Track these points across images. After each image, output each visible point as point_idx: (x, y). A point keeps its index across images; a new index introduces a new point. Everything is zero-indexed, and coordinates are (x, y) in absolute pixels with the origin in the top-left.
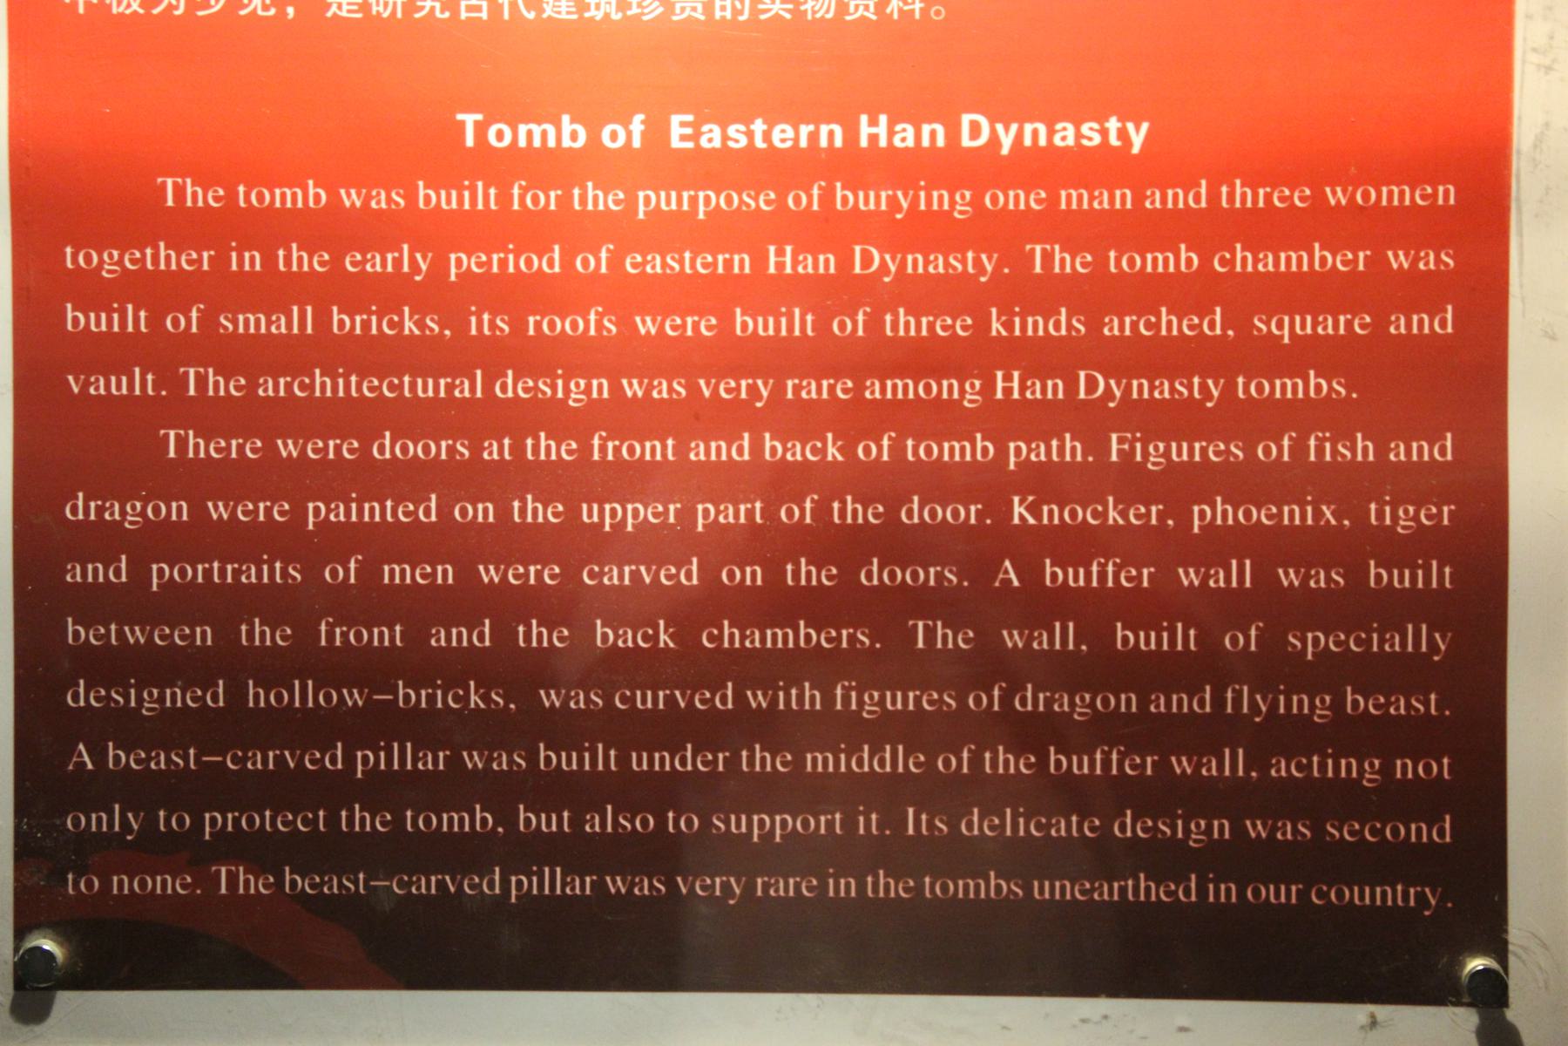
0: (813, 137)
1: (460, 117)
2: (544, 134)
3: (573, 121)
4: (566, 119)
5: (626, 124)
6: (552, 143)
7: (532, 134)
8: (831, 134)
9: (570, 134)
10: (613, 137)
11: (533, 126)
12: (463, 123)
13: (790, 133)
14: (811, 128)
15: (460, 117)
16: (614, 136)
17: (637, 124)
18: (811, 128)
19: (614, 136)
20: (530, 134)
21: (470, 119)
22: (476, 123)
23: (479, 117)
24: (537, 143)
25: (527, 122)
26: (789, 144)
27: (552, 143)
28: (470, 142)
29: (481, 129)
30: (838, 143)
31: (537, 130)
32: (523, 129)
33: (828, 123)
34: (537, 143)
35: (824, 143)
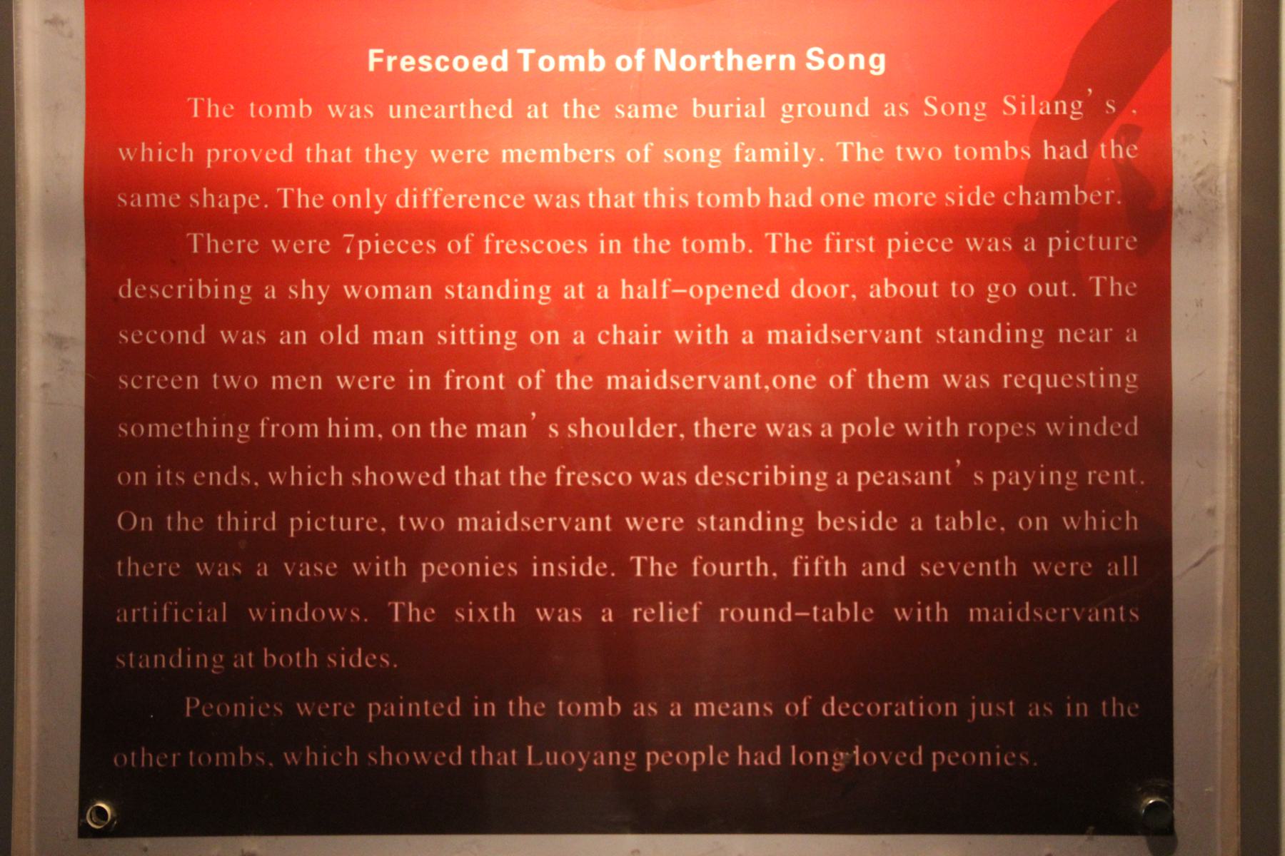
0: (775, 63)
1: (519, 51)
2: (577, 62)
3: (596, 54)
4: (591, 52)
5: (632, 54)
6: (582, 68)
7: (569, 62)
8: (788, 61)
9: (594, 62)
10: (624, 63)
11: (569, 57)
12: (521, 55)
13: (759, 60)
14: (774, 57)
15: (519, 51)
16: (624, 63)
17: (640, 55)
18: (774, 57)
19: (624, 63)
20: (567, 62)
21: (526, 53)
22: (531, 55)
23: (533, 51)
24: (572, 68)
25: (565, 54)
26: (758, 68)
27: (582, 68)
28: (526, 68)
29: (534, 60)
30: (792, 67)
31: (572, 59)
32: (562, 59)
33: (785, 53)
34: (572, 68)
35: (782, 67)
